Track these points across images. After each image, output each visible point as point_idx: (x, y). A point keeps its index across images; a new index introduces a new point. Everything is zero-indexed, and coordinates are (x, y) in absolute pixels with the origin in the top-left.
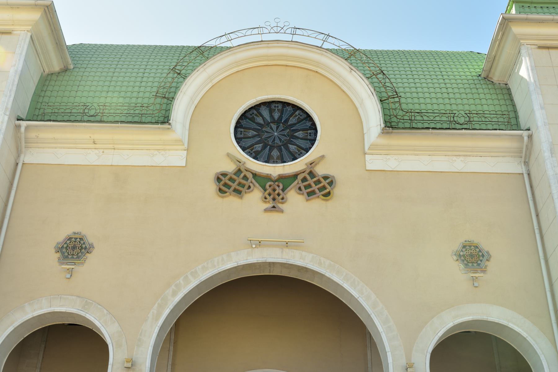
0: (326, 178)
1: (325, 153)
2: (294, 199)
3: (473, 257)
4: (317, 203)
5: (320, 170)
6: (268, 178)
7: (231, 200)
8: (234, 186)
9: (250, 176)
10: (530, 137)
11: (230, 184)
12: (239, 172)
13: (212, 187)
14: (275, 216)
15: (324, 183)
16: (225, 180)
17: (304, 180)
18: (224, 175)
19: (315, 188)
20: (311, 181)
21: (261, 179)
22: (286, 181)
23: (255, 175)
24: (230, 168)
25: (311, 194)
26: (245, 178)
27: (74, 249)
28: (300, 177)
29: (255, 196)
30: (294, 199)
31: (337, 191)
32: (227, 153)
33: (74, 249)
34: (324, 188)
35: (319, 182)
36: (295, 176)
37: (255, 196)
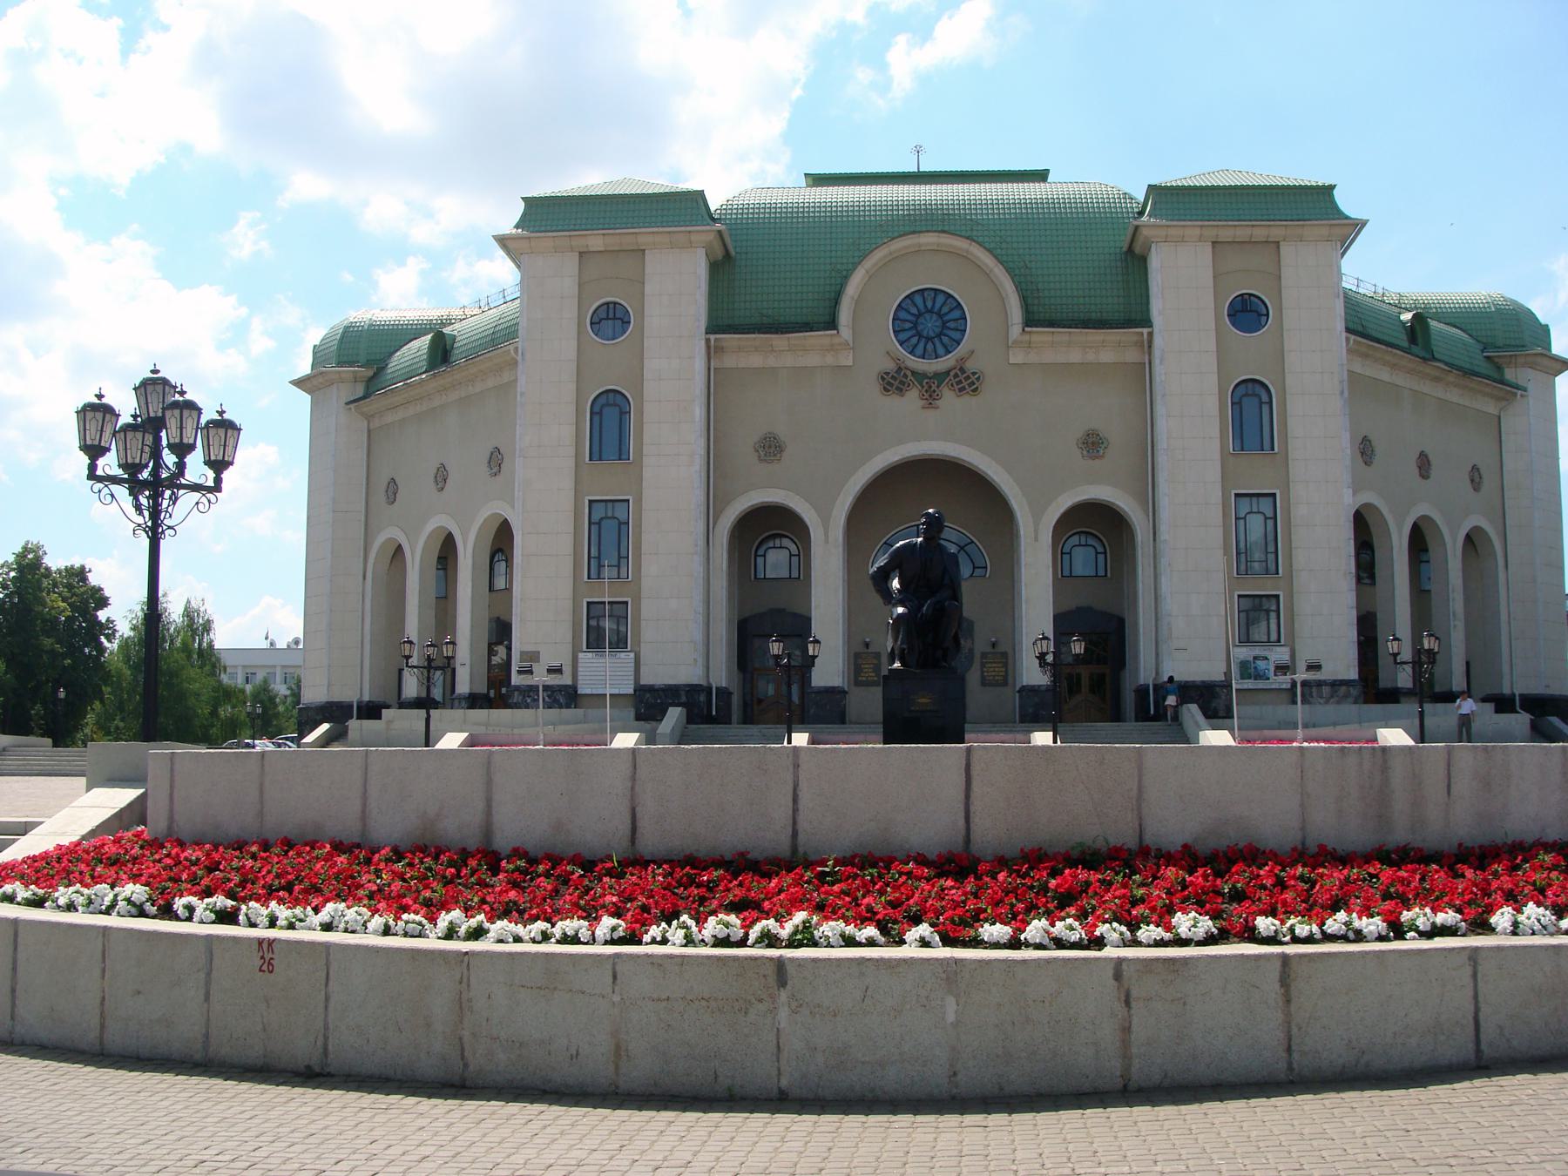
2: (948, 397)
3: (1093, 444)
4: (967, 401)
5: (970, 366)
6: (924, 375)
8: (896, 383)
10: (1151, 334)
12: (900, 369)
13: (875, 388)
14: (931, 412)
15: (973, 378)
16: (888, 378)
17: (956, 376)
20: (962, 377)
21: (919, 376)
22: (940, 377)
24: (890, 366)
25: (961, 390)
26: (905, 376)
27: (771, 448)
29: (913, 396)
30: (948, 397)
35: (968, 378)
36: (948, 373)
37: (913, 396)
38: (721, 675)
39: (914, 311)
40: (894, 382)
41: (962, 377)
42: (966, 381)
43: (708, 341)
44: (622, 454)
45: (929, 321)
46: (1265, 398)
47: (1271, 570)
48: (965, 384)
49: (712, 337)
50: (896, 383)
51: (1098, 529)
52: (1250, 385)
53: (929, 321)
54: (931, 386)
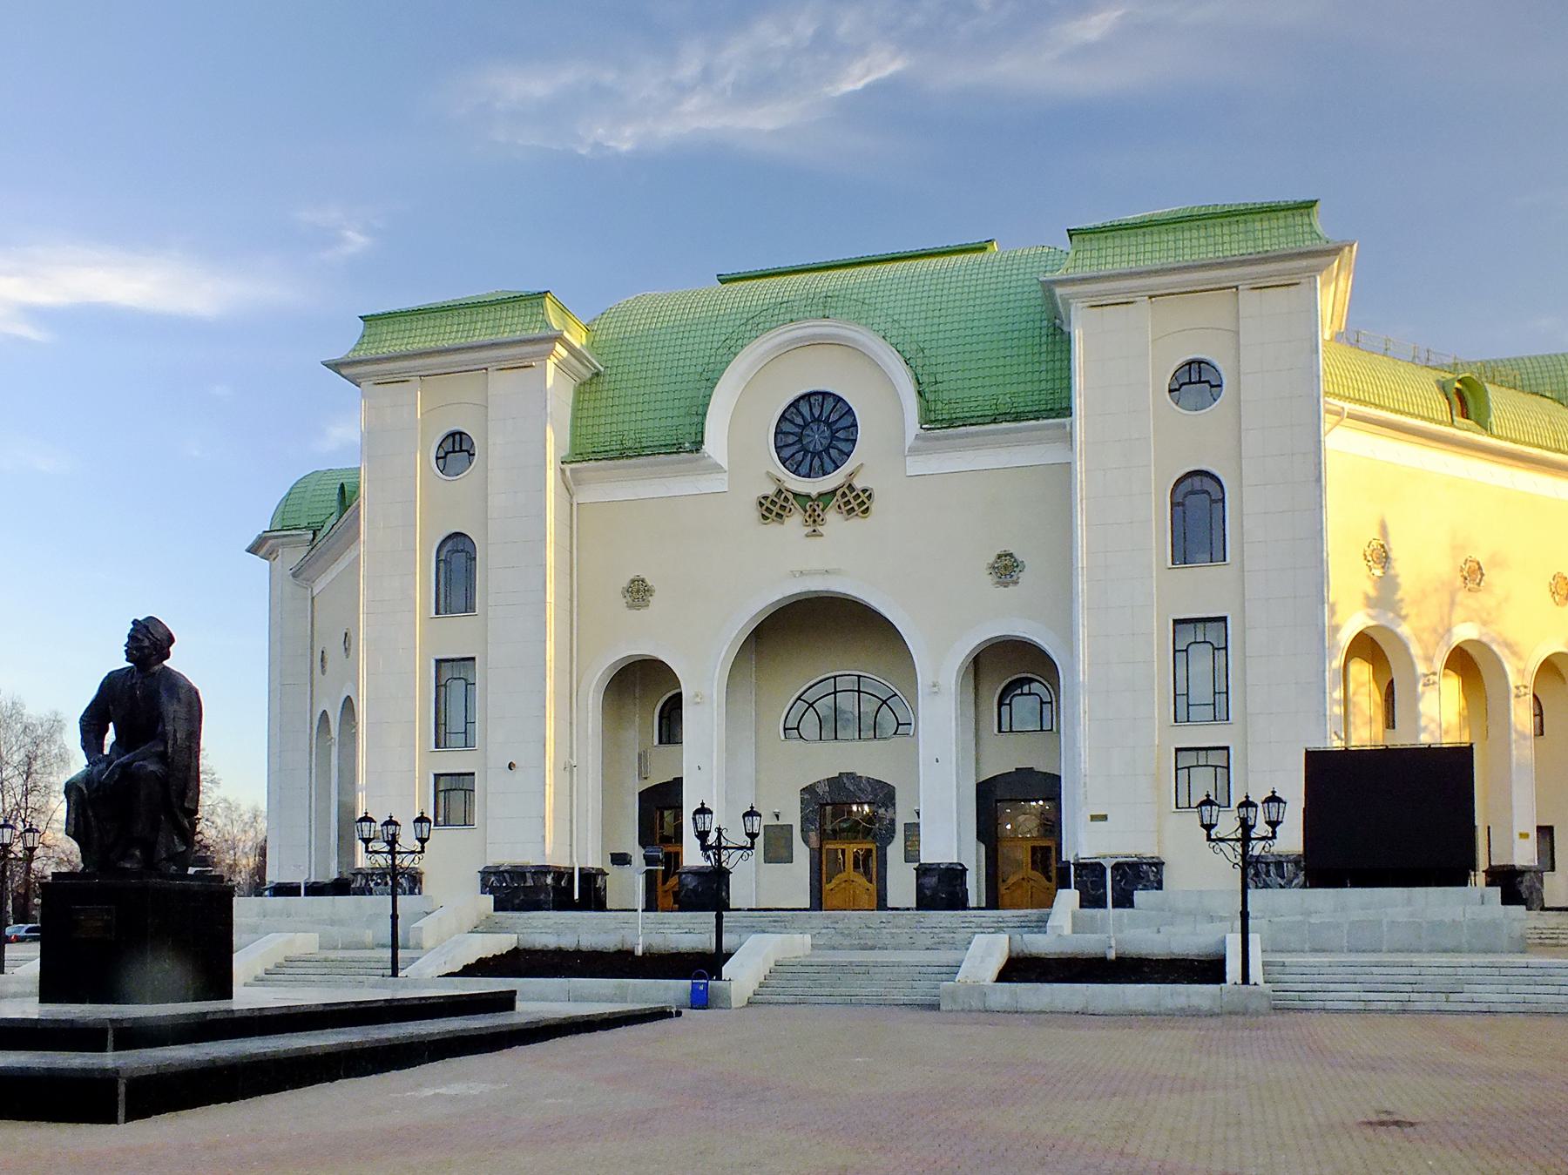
0: (864, 491)
1: (866, 462)
2: (833, 518)
3: (1006, 568)
4: (856, 523)
5: (859, 484)
6: (808, 496)
7: (773, 528)
9: (790, 497)
11: (773, 507)
13: (755, 513)
15: (863, 497)
16: (767, 504)
18: (766, 498)
19: (854, 504)
23: (796, 495)
24: (770, 490)
26: (786, 500)
27: (638, 592)
28: (839, 493)
29: (795, 522)
30: (833, 518)
31: (875, 506)
32: (767, 469)
33: (638, 592)
34: (863, 503)
36: (834, 492)
37: (795, 522)
38: (592, 857)
39: (799, 421)
40: (773, 507)
41: (850, 497)
42: (856, 502)
43: (563, 471)
44: (469, 608)
45: (816, 432)
46: (1216, 495)
47: (1219, 710)
48: (854, 504)
49: (567, 467)
50: (776, 509)
51: (1014, 672)
52: (1197, 479)
53: (816, 432)
54: (814, 508)
